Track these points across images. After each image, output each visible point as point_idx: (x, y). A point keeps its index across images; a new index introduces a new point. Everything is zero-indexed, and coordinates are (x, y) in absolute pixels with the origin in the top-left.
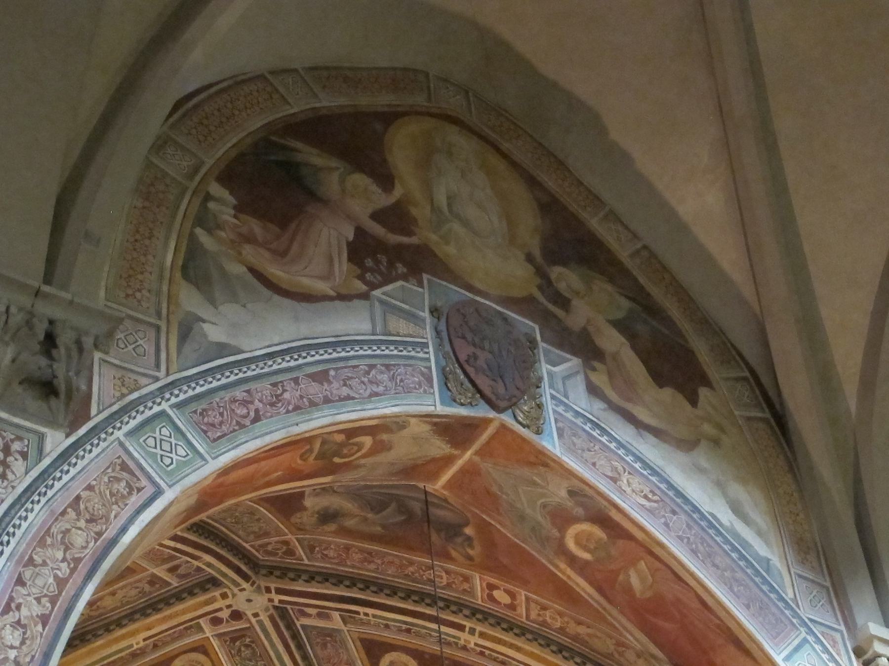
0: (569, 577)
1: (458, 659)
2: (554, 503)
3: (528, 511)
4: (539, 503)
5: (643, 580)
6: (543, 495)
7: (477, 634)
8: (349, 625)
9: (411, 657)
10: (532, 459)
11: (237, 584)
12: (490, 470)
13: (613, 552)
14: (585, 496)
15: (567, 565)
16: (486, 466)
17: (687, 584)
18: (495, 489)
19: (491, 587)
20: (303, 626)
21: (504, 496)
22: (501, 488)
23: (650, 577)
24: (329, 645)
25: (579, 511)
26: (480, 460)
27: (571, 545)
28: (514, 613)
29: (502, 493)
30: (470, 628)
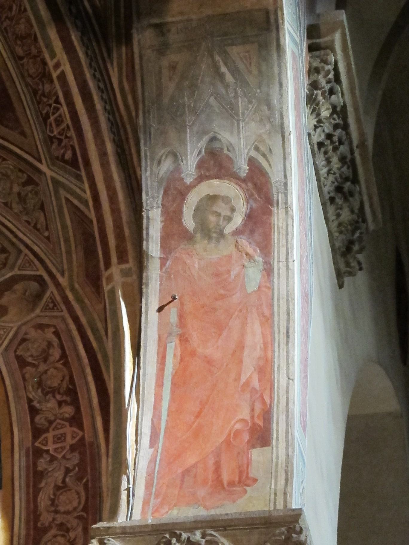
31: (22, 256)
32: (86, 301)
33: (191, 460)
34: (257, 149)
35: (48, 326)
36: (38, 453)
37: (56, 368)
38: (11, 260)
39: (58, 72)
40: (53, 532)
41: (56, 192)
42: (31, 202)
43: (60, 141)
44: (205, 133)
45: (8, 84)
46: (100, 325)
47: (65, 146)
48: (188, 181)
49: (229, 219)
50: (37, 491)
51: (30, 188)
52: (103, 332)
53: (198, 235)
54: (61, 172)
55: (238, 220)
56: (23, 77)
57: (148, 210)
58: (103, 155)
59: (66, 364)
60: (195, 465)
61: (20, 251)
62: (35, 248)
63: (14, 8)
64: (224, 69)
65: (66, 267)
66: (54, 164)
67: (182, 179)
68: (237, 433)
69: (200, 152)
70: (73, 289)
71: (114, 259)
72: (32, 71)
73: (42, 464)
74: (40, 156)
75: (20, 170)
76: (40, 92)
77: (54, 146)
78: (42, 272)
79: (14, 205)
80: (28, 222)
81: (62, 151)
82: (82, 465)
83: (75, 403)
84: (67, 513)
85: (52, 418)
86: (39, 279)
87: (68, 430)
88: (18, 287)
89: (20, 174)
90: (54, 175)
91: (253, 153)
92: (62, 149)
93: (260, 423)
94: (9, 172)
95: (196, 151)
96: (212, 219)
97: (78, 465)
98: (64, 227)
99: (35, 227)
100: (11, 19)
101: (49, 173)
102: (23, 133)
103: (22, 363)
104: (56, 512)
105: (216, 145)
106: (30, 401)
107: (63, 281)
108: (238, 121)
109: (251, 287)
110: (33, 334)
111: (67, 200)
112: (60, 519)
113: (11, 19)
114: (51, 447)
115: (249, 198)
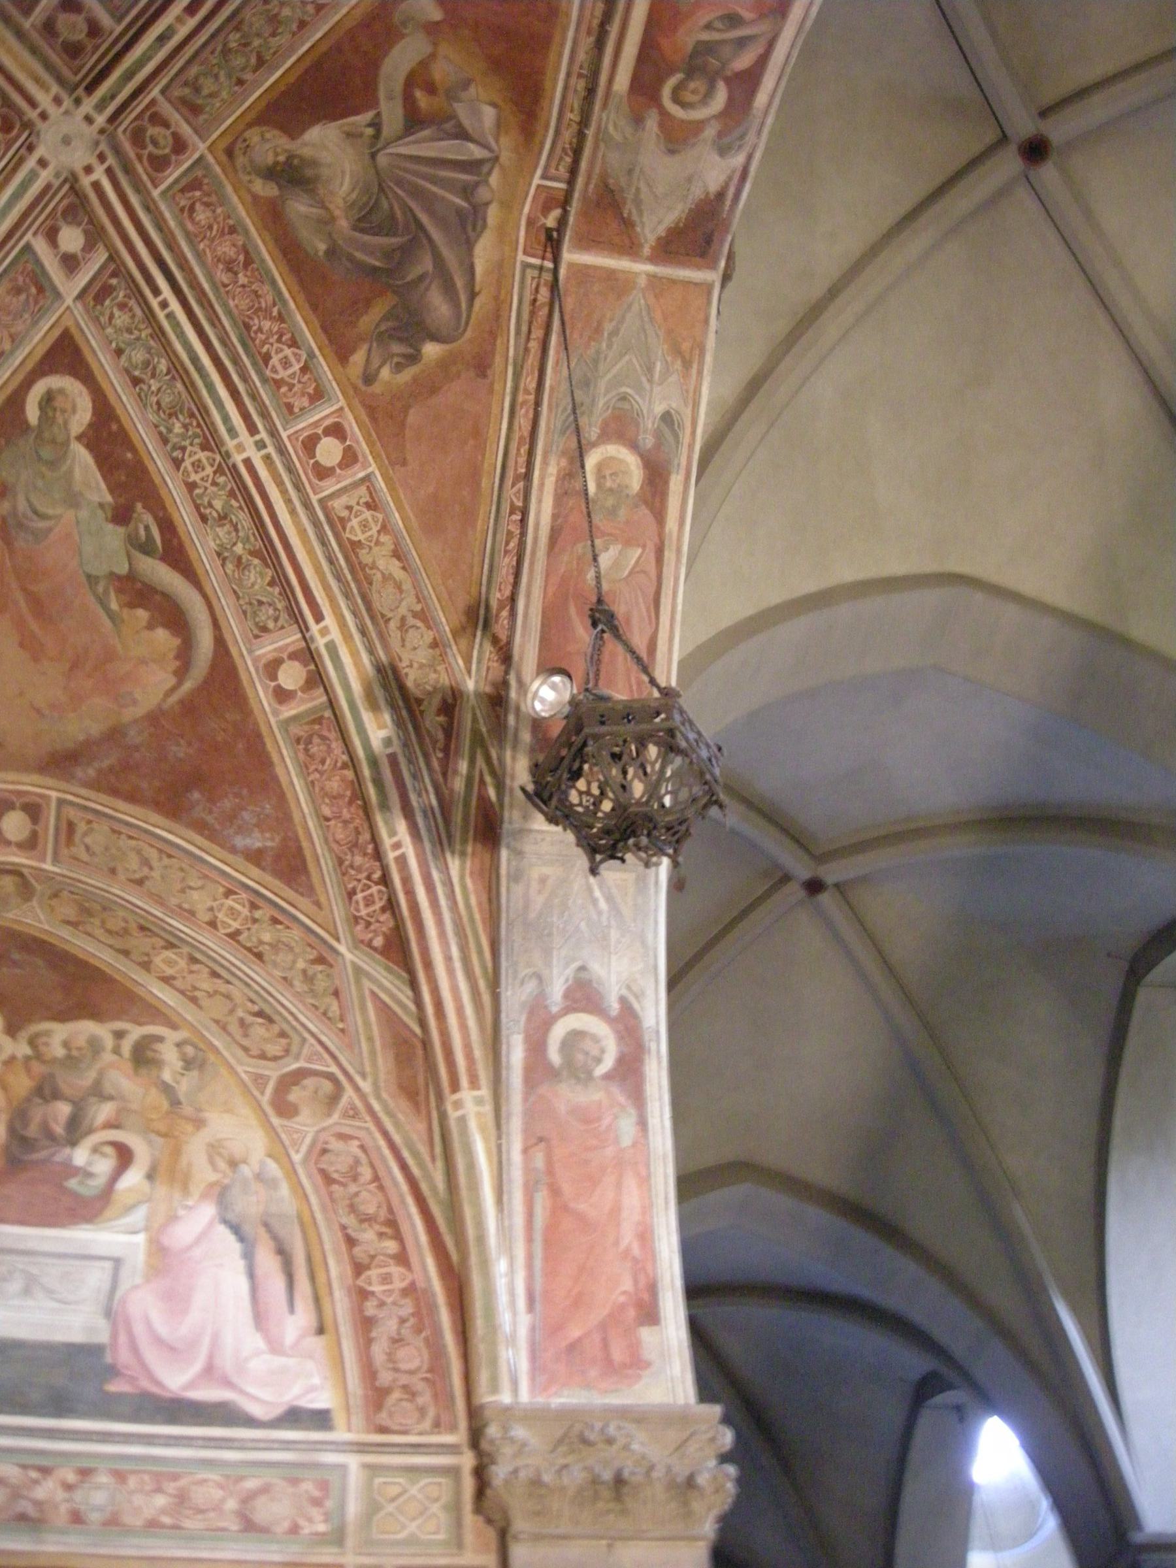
0: (542, 485)
1: (151, 468)
2: (636, 406)
3: (602, 384)
4: (623, 389)
5: (617, 564)
6: (639, 389)
7: (263, 452)
8: (79, 305)
9: (94, 408)
10: (686, 346)
11: (100, 107)
12: (635, 308)
13: (622, 513)
14: (676, 436)
15: (558, 474)
16: (638, 300)
17: (657, 618)
18: (608, 327)
19: (336, 431)
20: (28, 248)
21: (604, 345)
22: (615, 332)
23: (626, 573)
24: (23, 297)
25: (648, 441)
26: (643, 286)
27: (591, 461)
28: (315, 481)
29: (609, 338)
30: (262, 441)
31: (307, 1046)
32: (400, 1116)
33: (575, 1332)
34: (629, 988)
35: (351, 1137)
36: (363, 1295)
37: (369, 1191)
38: (294, 1049)
39: (398, 853)
40: (396, 1395)
41: (358, 982)
42: (321, 984)
43: (368, 924)
44: (574, 960)
45: (305, 844)
46: (423, 1150)
47: (375, 931)
48: (555, 1009)
49: (599, 1061)
50: (369, 1342)
51: (320, 968)
52: (427, 1158)
53: (565, 1073)
54: (365, 958)
55: (608, 1063)
56: (326, 840)
57: (508, 1037)
58: (448, 959)
59: (381, 1188)
60: (579, 1340)
61: (304, 1040)
62: (324, 1038)
63: (328, 761)
64: (597, 893)
65: (368, 1069)
66: (356, 948)
67: (546, 1007)
68: (622, 1307)
69: (567, 980)
70: (378, 1097)
71: (464, 1081)
72: (340, 836)
73: (370, 1308)
74: (337, 933)
75: (310, 945)
76: (347, 863)
77: (359, 928)
78: (334, 1069)
79: (297, 983)
80: (316, 1008)
81: (370, 935)
82: (417, 1314)
83: (398, 1236)
84: (411, 1372)
85: (372, 1253)
86: (331, 1077)
87: (396, 1270)
88: (309, 1082)
89: (309, 949)
90: (356, 960)
91: (624, 992)
92: (370, 932)
93: (646, 1296)
94: (293, 944)
95: (562, 980)
96: (580, 1057)
97: (413, 1315)
98: (367, 1023)
99: (325, 1014)
100: (321, 773)
101: (349, 956)
102: (318, 904)
103: (328, 1180)
104: (396, 1370)
105: (583, 975)
106: (344, 1228)
107: (366, 1086)
108: (610, 953)
109: (626, 1141)
110: (335, 1145)
111: (373, 993)
112: (404, 1379)
113: (321, 773)
114: (377, 1288)
115: (620, 1038)
